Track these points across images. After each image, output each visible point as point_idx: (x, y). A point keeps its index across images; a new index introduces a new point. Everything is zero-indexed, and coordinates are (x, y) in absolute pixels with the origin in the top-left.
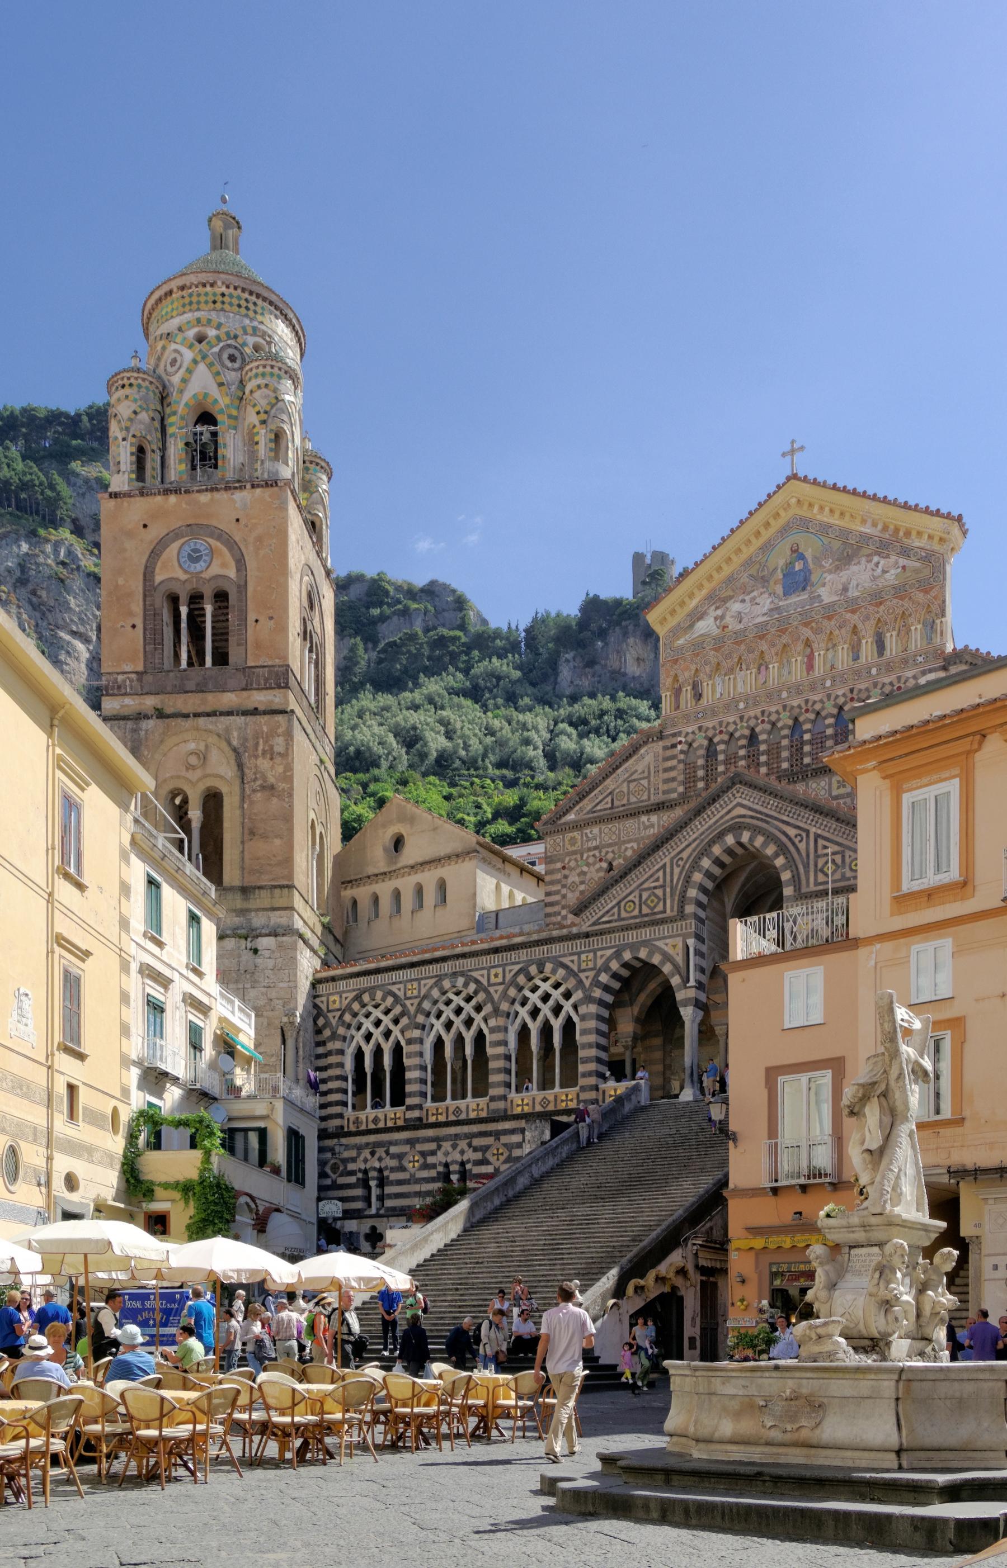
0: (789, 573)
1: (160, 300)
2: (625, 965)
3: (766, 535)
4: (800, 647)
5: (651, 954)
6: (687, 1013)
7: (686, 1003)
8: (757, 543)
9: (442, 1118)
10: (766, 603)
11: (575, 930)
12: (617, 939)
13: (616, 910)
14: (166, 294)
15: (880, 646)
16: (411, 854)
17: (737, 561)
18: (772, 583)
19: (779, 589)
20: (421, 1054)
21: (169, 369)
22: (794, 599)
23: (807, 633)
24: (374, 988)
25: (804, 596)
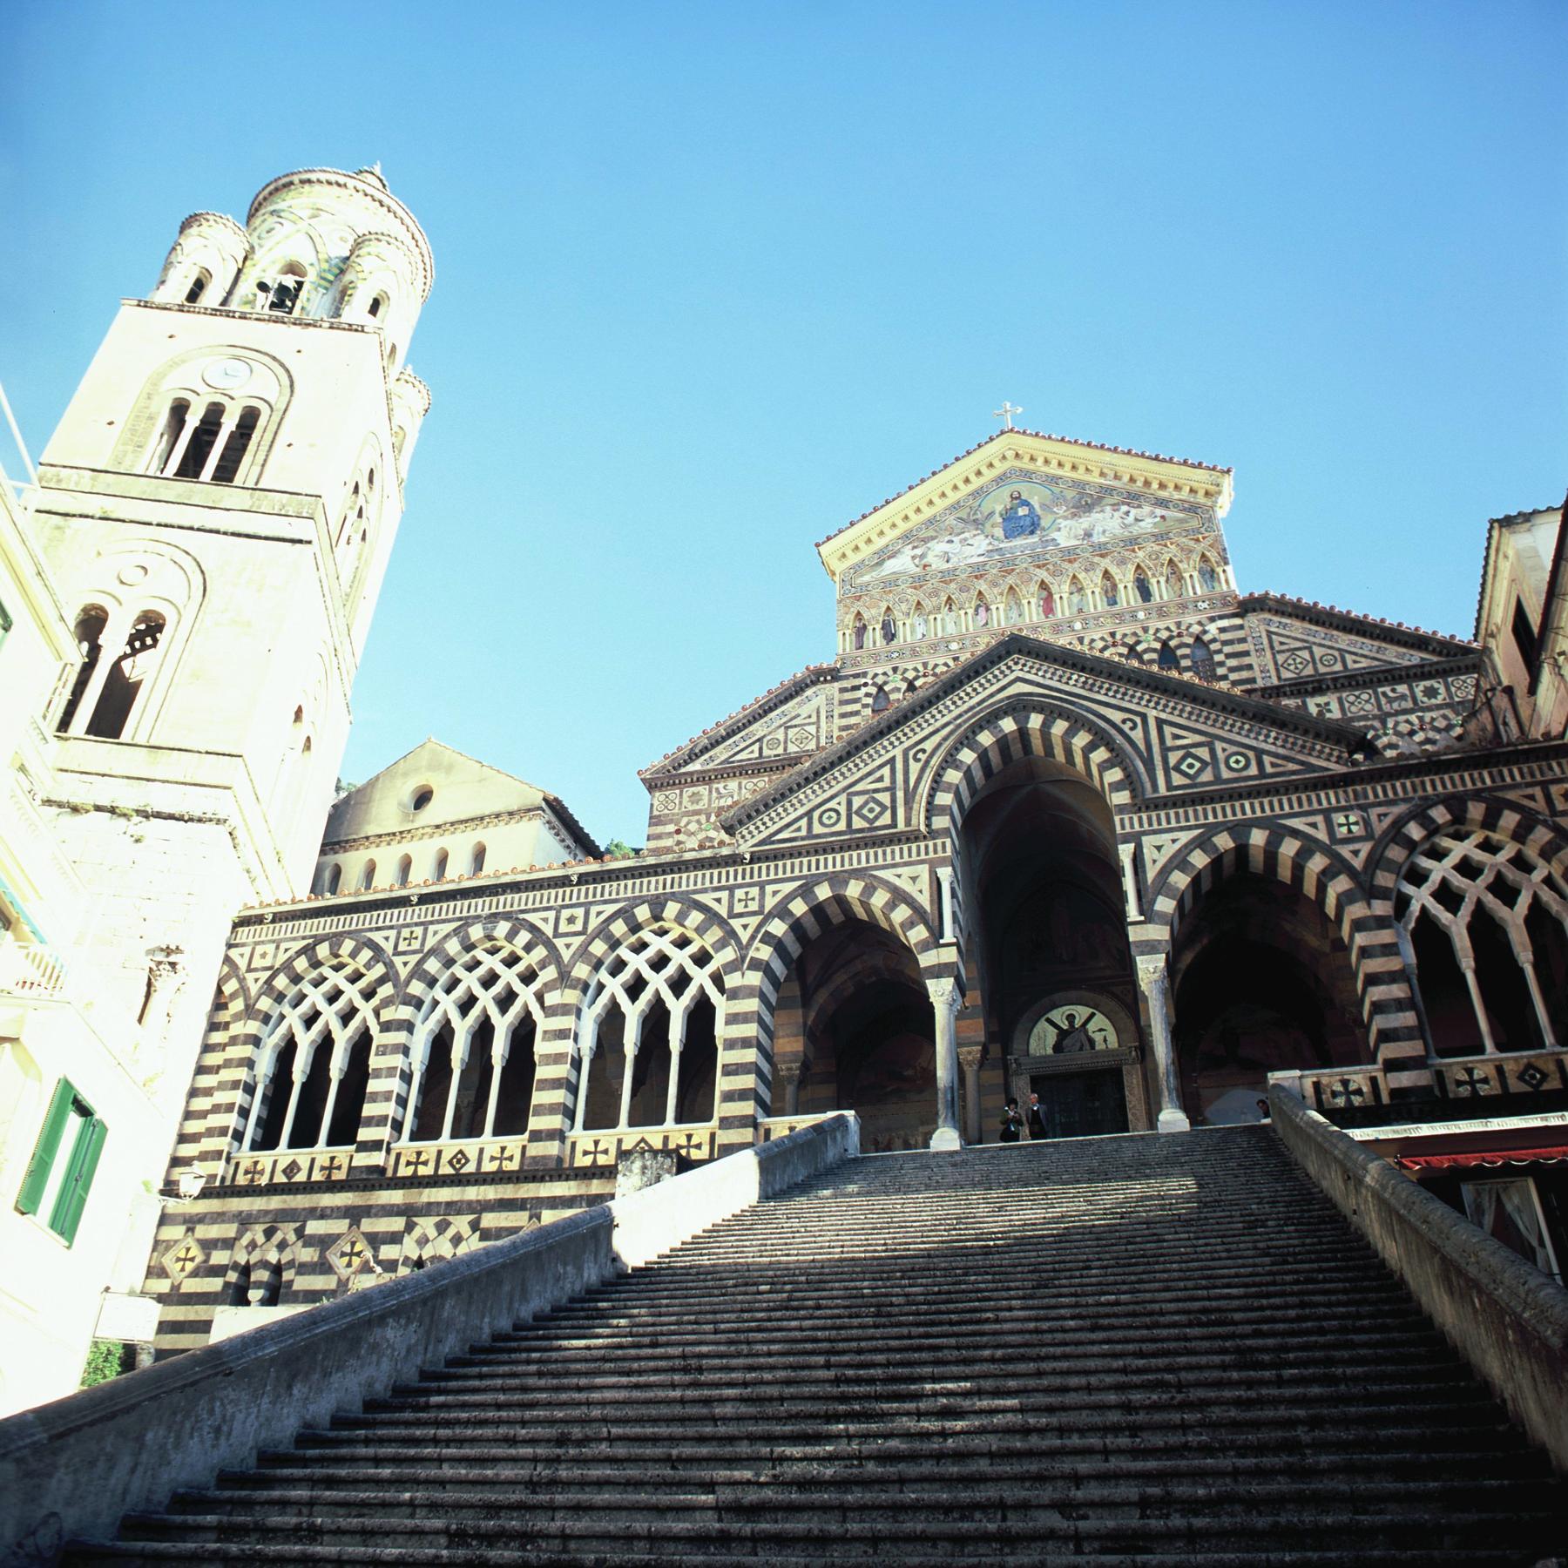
0: (1009, 517)
1: (277, 190)
2: (818, 910)
3: (976, 483)
4: (1034, 588)
5: (869, 890)
6: (940, 992)
7: (939, 971)
8: (965, 490)
9: (423, 1171)
10: (981, 544)
11: (725, 851)
12: (805, 866)
13: (804, 822)
14: (285, 186)
15: (1145, 592)
16: (433, 813)
17: (940, 504)
18: (988, 525)
19: (999, 532)
20: (406, 1051)
21: (264, 235)
22: (1019, 542)
23: (1042, 574)
24: (341, 934)
25: (1034, 539)
